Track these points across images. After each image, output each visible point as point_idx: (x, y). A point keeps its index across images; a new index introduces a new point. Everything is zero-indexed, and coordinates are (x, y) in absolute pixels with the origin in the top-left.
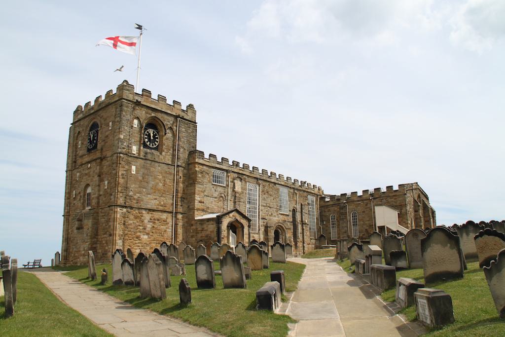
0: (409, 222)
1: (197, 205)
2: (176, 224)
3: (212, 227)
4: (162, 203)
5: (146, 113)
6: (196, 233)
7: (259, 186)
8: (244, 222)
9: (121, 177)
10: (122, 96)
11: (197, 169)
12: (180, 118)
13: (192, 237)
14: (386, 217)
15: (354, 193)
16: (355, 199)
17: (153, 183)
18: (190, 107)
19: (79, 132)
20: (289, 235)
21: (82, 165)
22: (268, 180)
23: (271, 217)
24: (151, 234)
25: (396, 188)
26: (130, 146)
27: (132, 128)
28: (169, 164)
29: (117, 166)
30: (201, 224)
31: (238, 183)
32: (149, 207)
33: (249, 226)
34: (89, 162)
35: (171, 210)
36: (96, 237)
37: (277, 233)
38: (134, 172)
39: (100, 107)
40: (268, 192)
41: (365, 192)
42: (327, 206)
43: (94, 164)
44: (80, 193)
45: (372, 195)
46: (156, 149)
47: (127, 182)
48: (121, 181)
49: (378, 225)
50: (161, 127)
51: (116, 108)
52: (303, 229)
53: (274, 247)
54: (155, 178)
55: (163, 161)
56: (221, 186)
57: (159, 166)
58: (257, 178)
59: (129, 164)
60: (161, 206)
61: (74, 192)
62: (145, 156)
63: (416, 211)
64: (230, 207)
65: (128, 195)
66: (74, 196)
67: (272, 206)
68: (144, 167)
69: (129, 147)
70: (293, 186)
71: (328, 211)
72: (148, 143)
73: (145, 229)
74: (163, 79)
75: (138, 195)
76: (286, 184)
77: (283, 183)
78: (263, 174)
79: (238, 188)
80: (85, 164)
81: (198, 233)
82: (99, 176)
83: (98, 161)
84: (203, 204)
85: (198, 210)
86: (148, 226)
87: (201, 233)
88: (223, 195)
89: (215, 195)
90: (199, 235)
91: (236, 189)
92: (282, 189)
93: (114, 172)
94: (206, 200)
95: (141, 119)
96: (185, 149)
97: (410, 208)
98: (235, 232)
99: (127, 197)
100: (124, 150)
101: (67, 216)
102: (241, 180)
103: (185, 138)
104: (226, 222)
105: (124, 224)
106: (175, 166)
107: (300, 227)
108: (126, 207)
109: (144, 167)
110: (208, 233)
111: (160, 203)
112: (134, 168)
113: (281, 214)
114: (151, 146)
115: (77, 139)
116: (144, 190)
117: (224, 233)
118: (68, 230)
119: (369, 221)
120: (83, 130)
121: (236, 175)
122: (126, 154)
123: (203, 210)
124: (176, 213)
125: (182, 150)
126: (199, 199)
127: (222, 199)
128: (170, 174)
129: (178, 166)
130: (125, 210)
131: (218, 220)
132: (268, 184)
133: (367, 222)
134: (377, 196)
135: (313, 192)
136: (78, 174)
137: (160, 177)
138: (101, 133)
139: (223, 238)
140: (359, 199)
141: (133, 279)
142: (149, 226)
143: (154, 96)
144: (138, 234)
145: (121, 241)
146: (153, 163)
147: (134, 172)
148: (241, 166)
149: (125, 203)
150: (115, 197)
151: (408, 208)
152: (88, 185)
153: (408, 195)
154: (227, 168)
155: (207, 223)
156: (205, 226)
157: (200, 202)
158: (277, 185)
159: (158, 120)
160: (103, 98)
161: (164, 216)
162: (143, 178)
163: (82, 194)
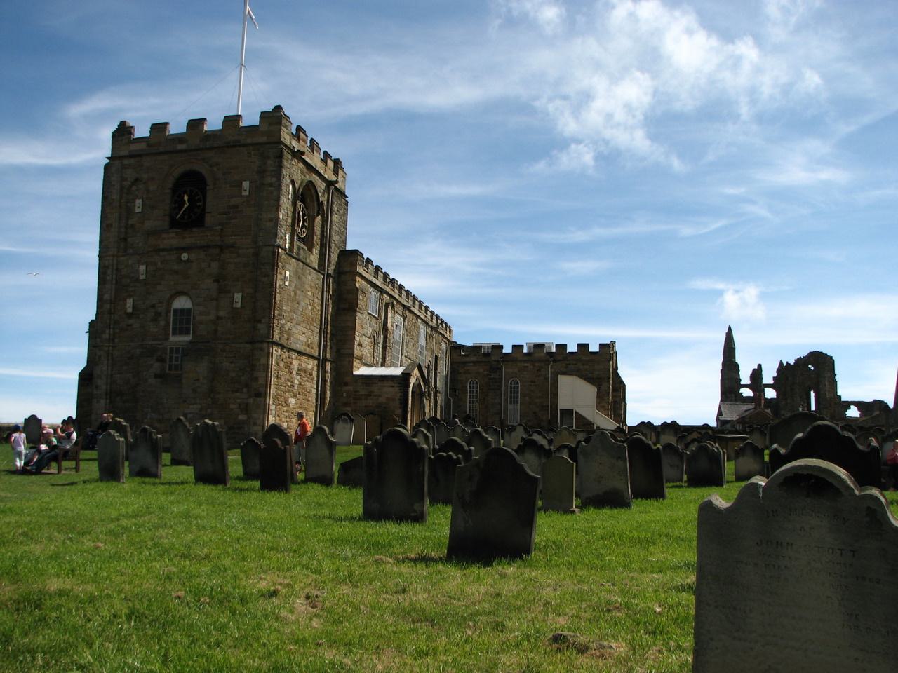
3: (392, 391)
25: (594, 348)
35: (316, 354)
49: (560, 407)
50: (313, 201)
71: (465, 373)
87: (366, 399)
93: (265, 279)
106: (324, 275)
110: (382, 400)
111: (308, 341)
133: (537, 400)
155: (380, 384)
156: (375, 389)
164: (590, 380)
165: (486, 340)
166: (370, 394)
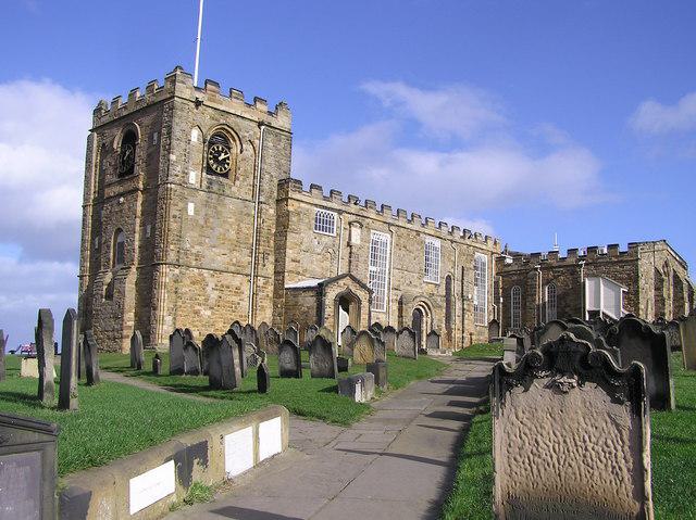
1: (289, 265)
3: (309, 301)
4: (234, 260)
8: (362, 294)
11: (290, 208)
15: (553, 254)
22: (409, 226)
32: (214, 266)
33: (370, 302)
34: (121, 195)
41: (572, 252)
45: (582, 258)
46: (226, 175)
48: (174, 226)
59: (183, 199)
60: (234, 265)
62: (209, 187)
63: (658, 289)
64: (343, 270)
73: (207, 300)
75: (198, 248)
76: (438, 234)
79: (356, 240)
86: (212, 296)
89: (319, 251)
91: (353, 241)
98: (347, 310)
102: (361, 226)
104: (331, 294)
107: (458, 305)
109: (207, 204)
112: (191, 207)
117: (329, 311)
121: (353, 218)
130: (177, 271)
131: (319, 291)
135: (484, 247)
142: (214, 295)
144: (197, 307)
145: (171, 318)
151: (642, 282)
161: (237, 281)
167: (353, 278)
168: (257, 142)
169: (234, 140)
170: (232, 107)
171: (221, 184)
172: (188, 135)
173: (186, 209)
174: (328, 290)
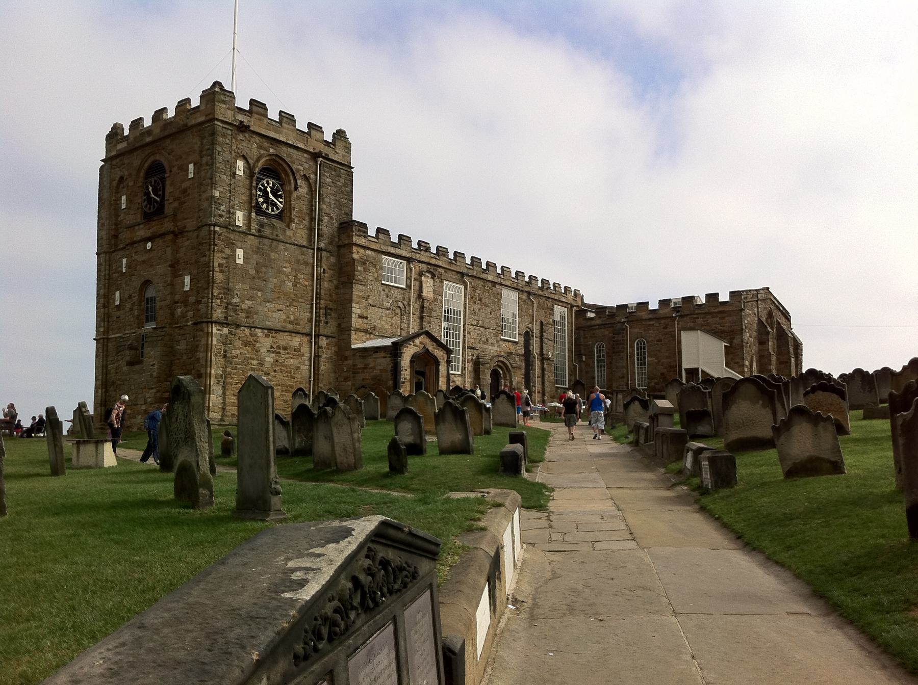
0: (747, 363)
1: (356, 322)
2: (317, 356)
3: (384, 362)
4: (292, 317)
5: (260, 147)
6: (354, 373)
7: (466, 288)
8: (439, 353)
9: (217, 270)
10: (213, 113)
11: (355, 256)
12: (323, 157)
13: (346, 379)
14: (702, 353)
16: (644, 315)
17: (275, 281)
18: (340, 135)
19: (122, 178)
20: (518, 379)
21: (133, 243)
22: (484, 276)
23: (486, 347)
24: (273, 374)
25: (724, 297)
26: (232, 211)
27: (234, 178)
28: (304, 247)
29: (209, 250)
30: (363, 357)
31: (428, 284)
32: (269, 324)
33: (449, 362)
35: (307, 330)
36: (170, 379)
37: (495, 374)
38: (240, 261)
39: (166, 133)
40: (480, 300)
41: (664, 303)
42: (590, 328)
43: (159, 242)
44: (130, 297)
45: (676, 309)
46: (280, 217)
47: (228, 279)
48: (218, 277)
49: (686, 365)
51: (202, 138)
52: (543, 370)
53: (497, 400)
54: (280, 272)
55: (293, 240)
56: (398, 288)
57: (285, 249)
58: (463, 274)
59: (232, 245)
60: (291, 322)
61: (117, 294)
63: (762, 342)
64: (413, 329)
65: (230, 304)
66: (117, 303)
67: (486, 325)
68: (258, 250)
69: (231, 214)
70: (527, 289)
72: (265, 205)
73: (261, 364)
74: (294, 83)
75: (249, 303)
77: (509, 284)
78: (472, 264)
79: (428, 292)
80: (140, 241)
81: (358, 373)
82: (171, 266)
83: (170, 237)
84: (365, 321)
85: (357, 330)
86: (268, 359)
87: (363, 372)
88: (400, 305)
89: (387, 304)
90: (360, 377)
91: (425, 294)
92: (505, 292)
94: (370, 312)
95: (250, 161)
96: (331, 218)
97: (749, 337)
99: (230, 307)
100: (222, 219)
101: (103, 341)
102: (433, 276)
103: (332, 197)
105: (225, 356)
107: (537, 363)
108: (228, 324)
109: (258, 250)
111: (288, 317)
112: (240, 252)
113: (505, 340)
114: (270, 211)
115: (117, 192)
116: (260, 294)
118: (107, 366)
119: (667, 357)
120: (130, 175)
122: (226, 228)
123: (366, 331)
124: (317, 336)
125: (326, 219)
126: (359, 311)
127: (398, 311)
128: (306, 263)
129: (319, 249)
130: (225, 330)
131: (395, 350)
132: (481, 283)
134: (686, 312)
136: (124, 261)
137: (289, 270)
138: (172, 184)
139: (403, 382)
140: (651, 316)
141: (287, 446)
142: (269, 359)
143: (273, 115)
146: (275, 243)
147: (240, 261)
148: (434, 250)
149: (226, 318)
150: (208, 307)
151: (746, 336)
152: (147, 283)
153: (747, 311)
154: (408, 255)
155: (375, 355)
156: (371, 361)
157: (360, 317)
158: (498, 286)
159: (281, 162)
160: (171, 113)
161: (296, 341)
162: (257, 272)
163: (135, 299)
164: (718, 334)
165: (631, 299)
166: (366, 367)
167: (428, 335)
168: (312, 176)
169: (287, 175)
170: (280, 133)
171: (273, 227)
172: (233, 166)
173: (234, 256)
174: (405, 350)
